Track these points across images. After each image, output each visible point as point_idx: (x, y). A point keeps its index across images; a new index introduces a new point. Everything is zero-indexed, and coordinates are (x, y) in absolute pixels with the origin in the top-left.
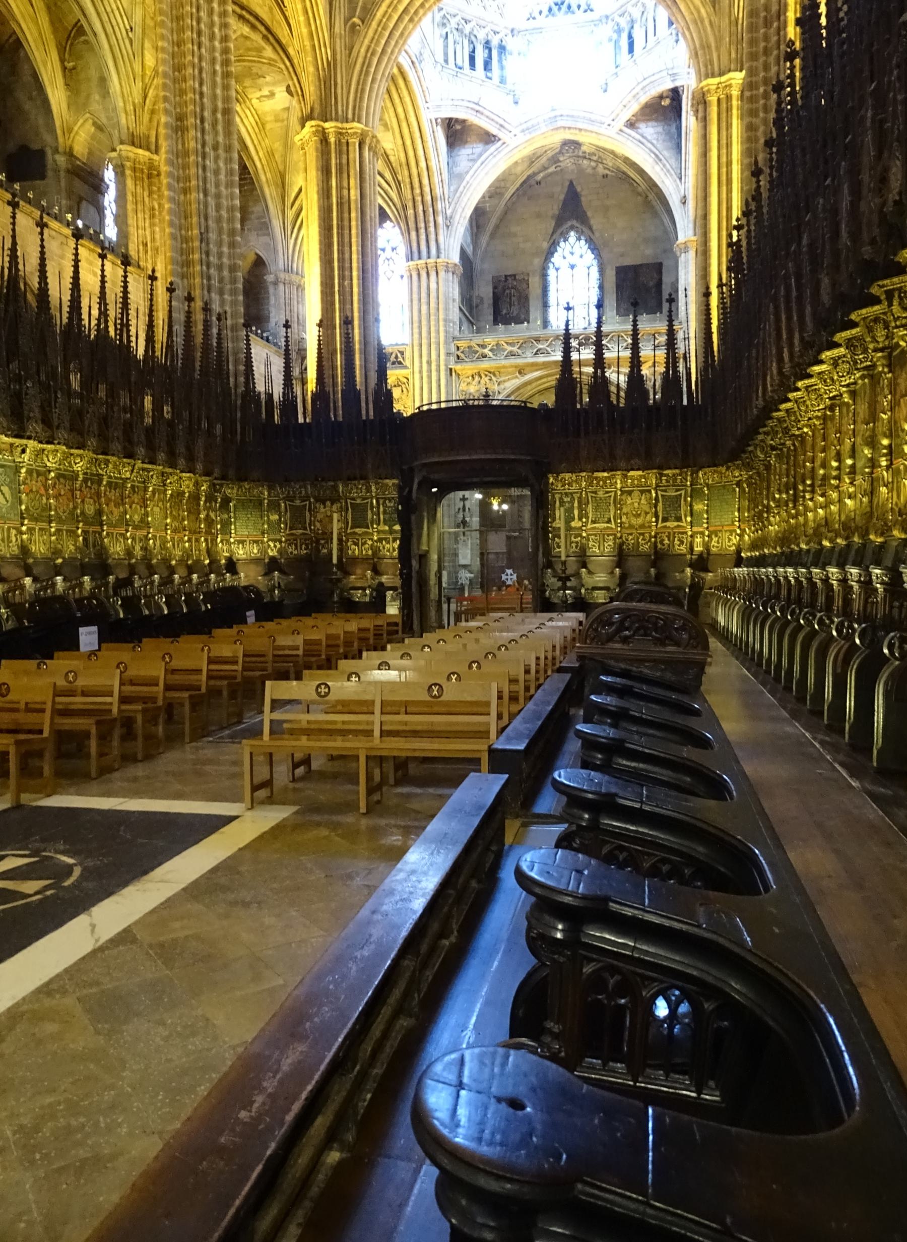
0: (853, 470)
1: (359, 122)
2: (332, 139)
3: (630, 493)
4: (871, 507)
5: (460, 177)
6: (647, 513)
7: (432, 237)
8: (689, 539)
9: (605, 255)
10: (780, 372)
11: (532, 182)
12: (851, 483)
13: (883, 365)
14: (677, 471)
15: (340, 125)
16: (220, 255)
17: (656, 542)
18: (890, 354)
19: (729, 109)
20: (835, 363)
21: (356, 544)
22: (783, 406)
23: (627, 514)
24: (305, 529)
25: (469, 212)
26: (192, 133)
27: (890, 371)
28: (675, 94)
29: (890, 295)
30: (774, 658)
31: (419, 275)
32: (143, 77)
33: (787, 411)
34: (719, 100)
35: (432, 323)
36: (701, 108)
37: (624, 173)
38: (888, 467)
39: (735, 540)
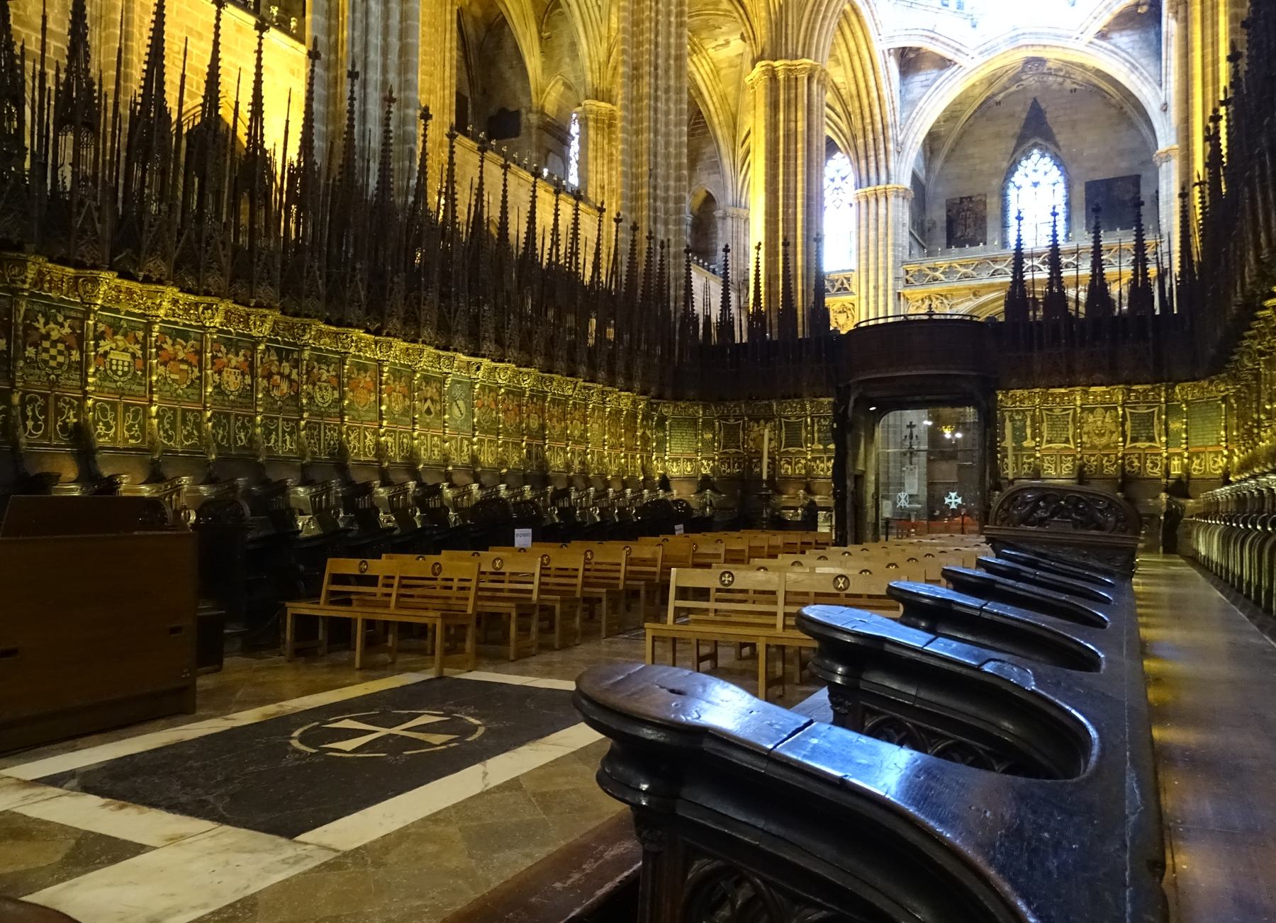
1: (808, 57)
2: (781, 76)
3: (1092, 410)
5: (913, 103)
6: (1112, 433)
7: (882, 164)
8: (1165, 461)
9: (1074, 170)
11: (991, 102)
14: (1149, 387)
15: (789, 62)
16: (667, 189)
17: (1123, 464)
21: (790, 463)
23: (1088, 433)
24: (738, 447)
25: (922, 137)
26: (646, 79)
30: (1255, 579)
31: (867, 202)
32: (608, 38)
35: (880, 248)
36: (1181, 9)
37: (1095, 86)
39: (1222, 462)
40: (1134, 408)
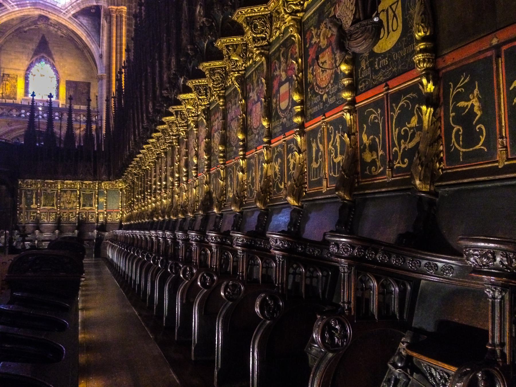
0: (166, 187)
3: (65, 192)
4: (172, 203)
6: (74, 202)
8: (97, 215)
10: (135, 140)
12: (165, 192)
13: (175, 142)
14: (91, 182)
17: (79, 217)
18: (179, 138)
19: (121, 21)
20: (158, 139)
22: (138, 156)
23: (63, 202)
27: (179, 145)
28: (98, 8)
29: (177, 112)
33: (140, 158)
34: (117, 16)
38: (178, 186)
39: (119, 216)
40: (84, 191)
